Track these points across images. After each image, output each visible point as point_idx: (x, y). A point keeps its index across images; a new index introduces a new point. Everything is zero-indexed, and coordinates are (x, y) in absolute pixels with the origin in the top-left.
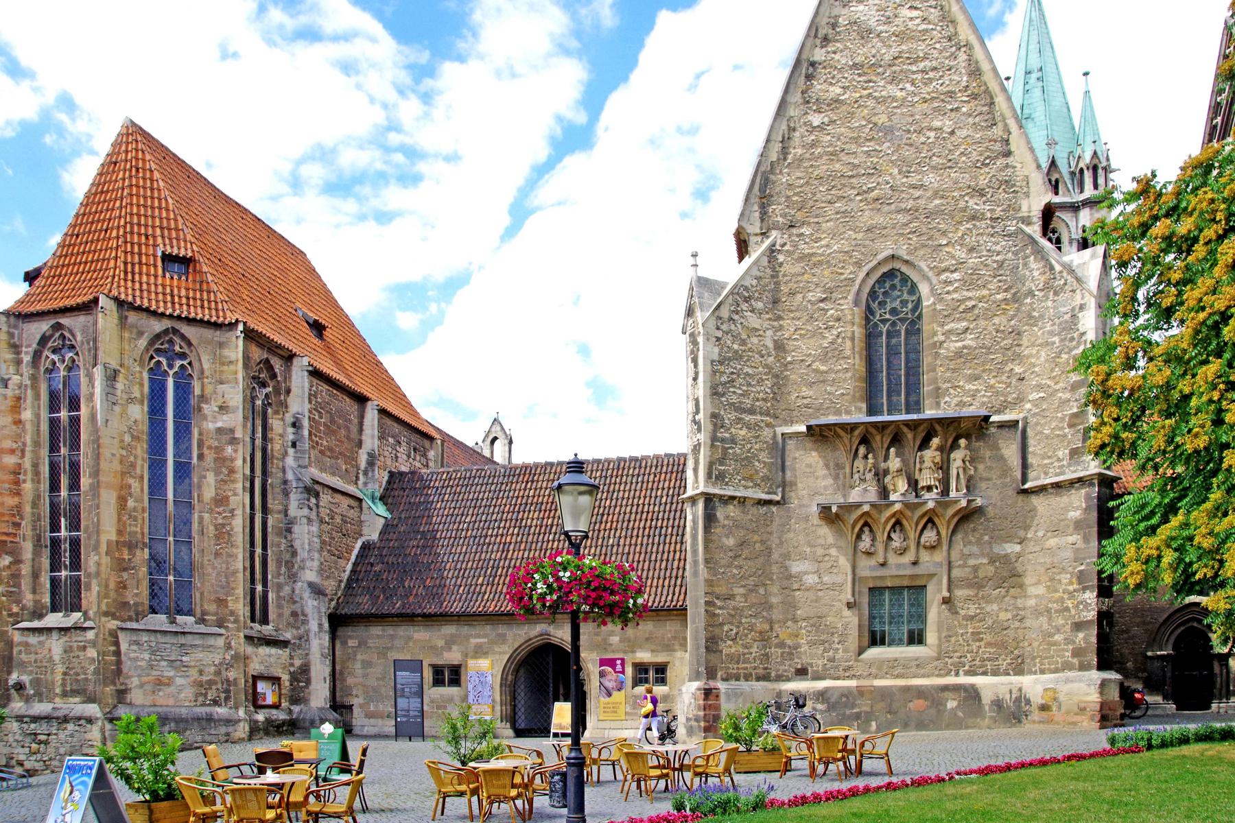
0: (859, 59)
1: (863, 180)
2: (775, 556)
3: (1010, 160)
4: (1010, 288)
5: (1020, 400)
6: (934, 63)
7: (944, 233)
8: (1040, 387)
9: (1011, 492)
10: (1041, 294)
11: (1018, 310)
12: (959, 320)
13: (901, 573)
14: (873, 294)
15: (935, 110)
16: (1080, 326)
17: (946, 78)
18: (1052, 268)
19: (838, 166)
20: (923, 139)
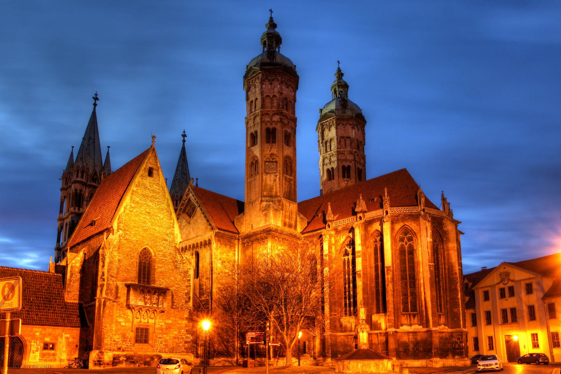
0: (144, 193)
1: (142, 224)
2: (115, 316)
3: (174, 229)
4: (172, 259)
5: (173, 286)
6: (160, 201)
7: (159, 242)
8: (177, 284)
9: (170, 308)
10: (179, 263)
11: (173, 265)
12: (161, 264)
13: (145, 324)
14: (141, 253)
15: (159, 212)
16: (189, 273)
17: (162, 205)
18: (183, 258)
19: (137, 219)
20: (156, 218)
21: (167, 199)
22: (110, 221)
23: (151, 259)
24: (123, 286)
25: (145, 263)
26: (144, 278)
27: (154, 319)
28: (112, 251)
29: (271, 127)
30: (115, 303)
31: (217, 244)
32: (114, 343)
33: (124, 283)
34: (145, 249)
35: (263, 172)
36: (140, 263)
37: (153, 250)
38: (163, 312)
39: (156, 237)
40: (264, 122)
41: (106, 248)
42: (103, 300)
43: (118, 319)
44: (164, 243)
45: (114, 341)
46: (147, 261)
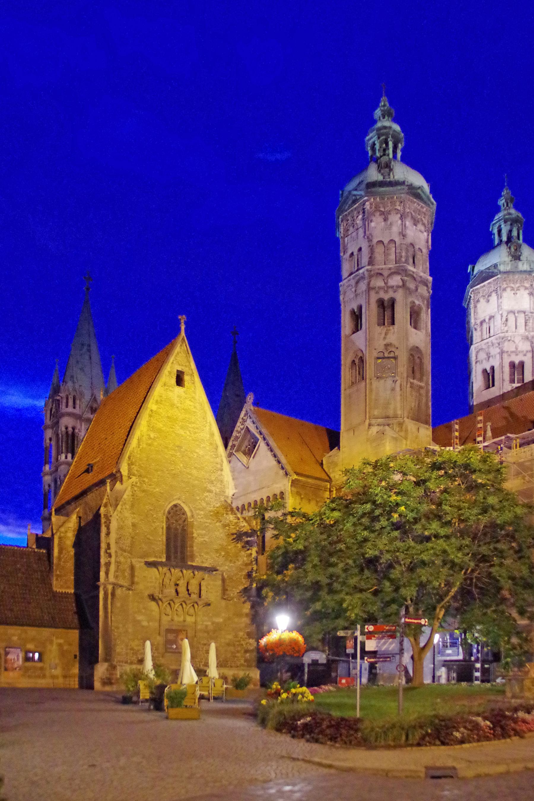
3: (223, 473)
7: (198, 495)
17: (202, 434)
21: (210, 423)
22: (115, 462)
23: (186, 523)
24: (143, 564)
25: (176, 529)
26: (176, 552)
27: (194, 616)
28: (122, 509)
29: (386, 297)
30: (131, 592)
31: (295, 499)
32: (132, 652)
33: (143, 560)
34: (175, 506)
35: (373, 375)
36: (168, 528)
37: (189, 507)
38: (209, 605)
39: (193, 486)
40: (374, 288)
41: (111, 506)
42: (110, 588)
43: (136, 615)
44: (207, 496)
45: (132, 649)
46: (180, 525)
